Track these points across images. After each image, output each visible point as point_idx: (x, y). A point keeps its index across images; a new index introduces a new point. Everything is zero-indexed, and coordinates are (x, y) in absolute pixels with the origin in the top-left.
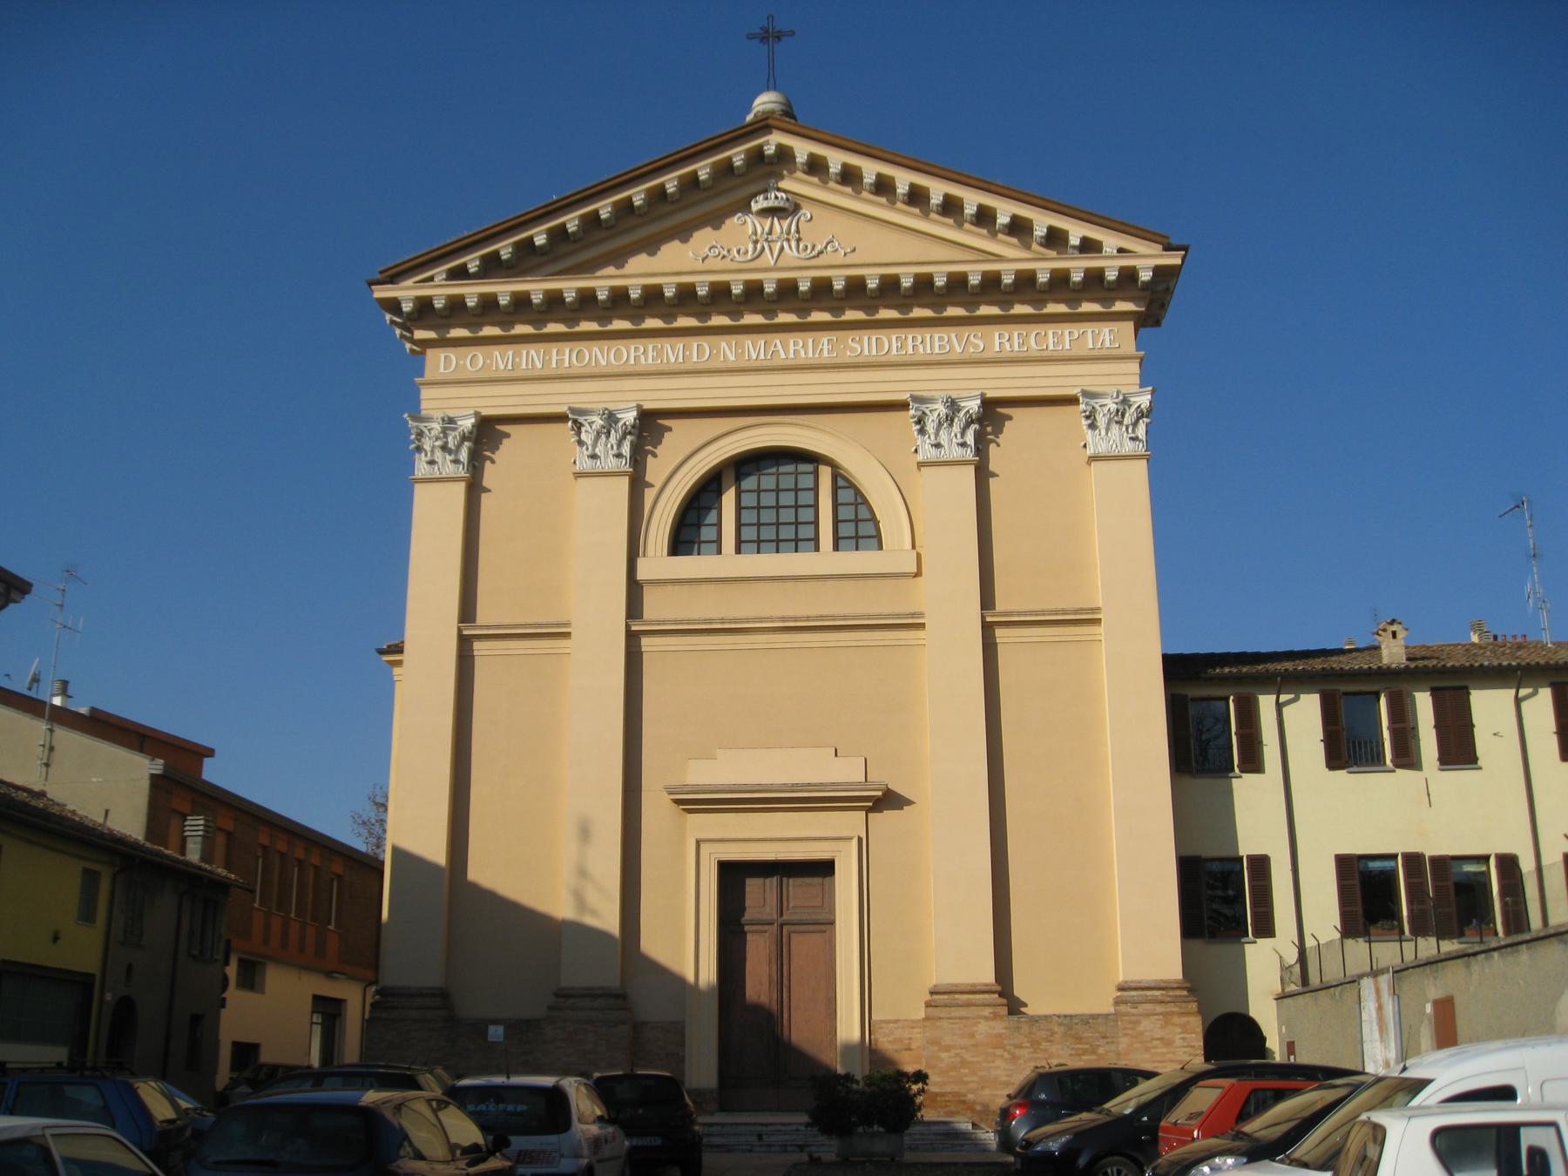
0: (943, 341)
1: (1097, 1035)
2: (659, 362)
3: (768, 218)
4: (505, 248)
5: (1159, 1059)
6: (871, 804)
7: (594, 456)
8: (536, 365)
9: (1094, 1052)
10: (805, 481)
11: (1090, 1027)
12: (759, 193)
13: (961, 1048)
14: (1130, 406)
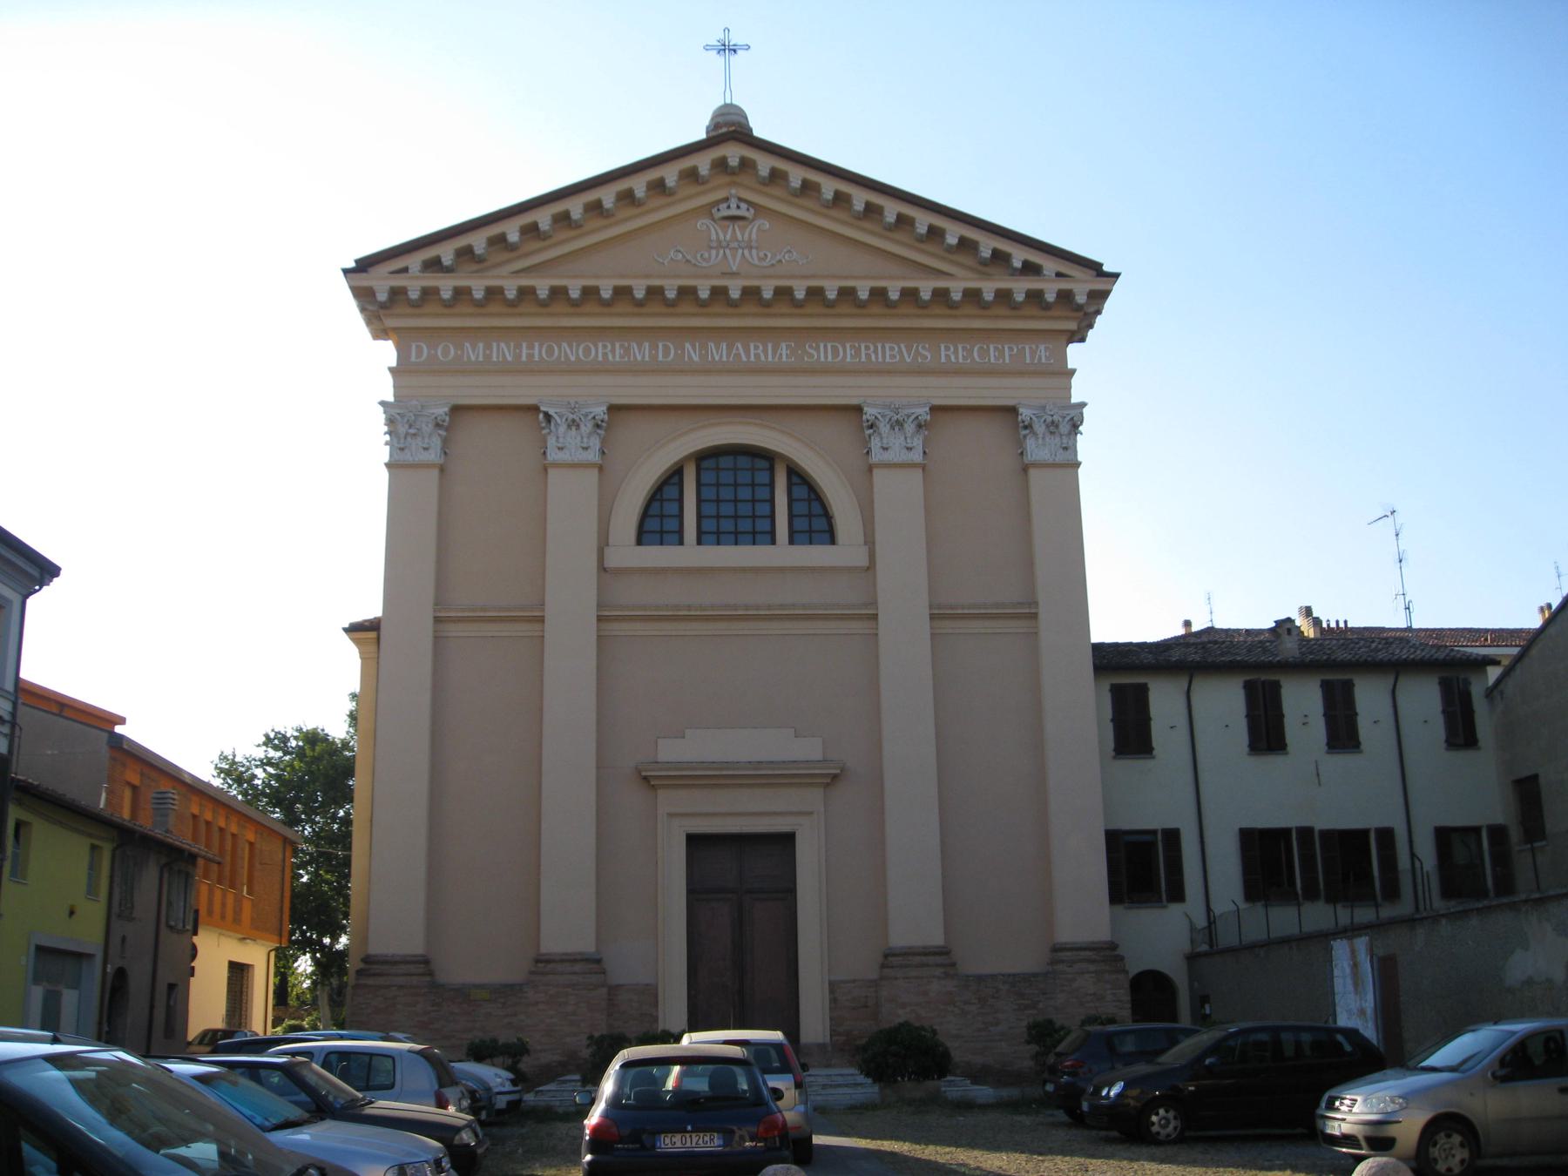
10: (763, 477)
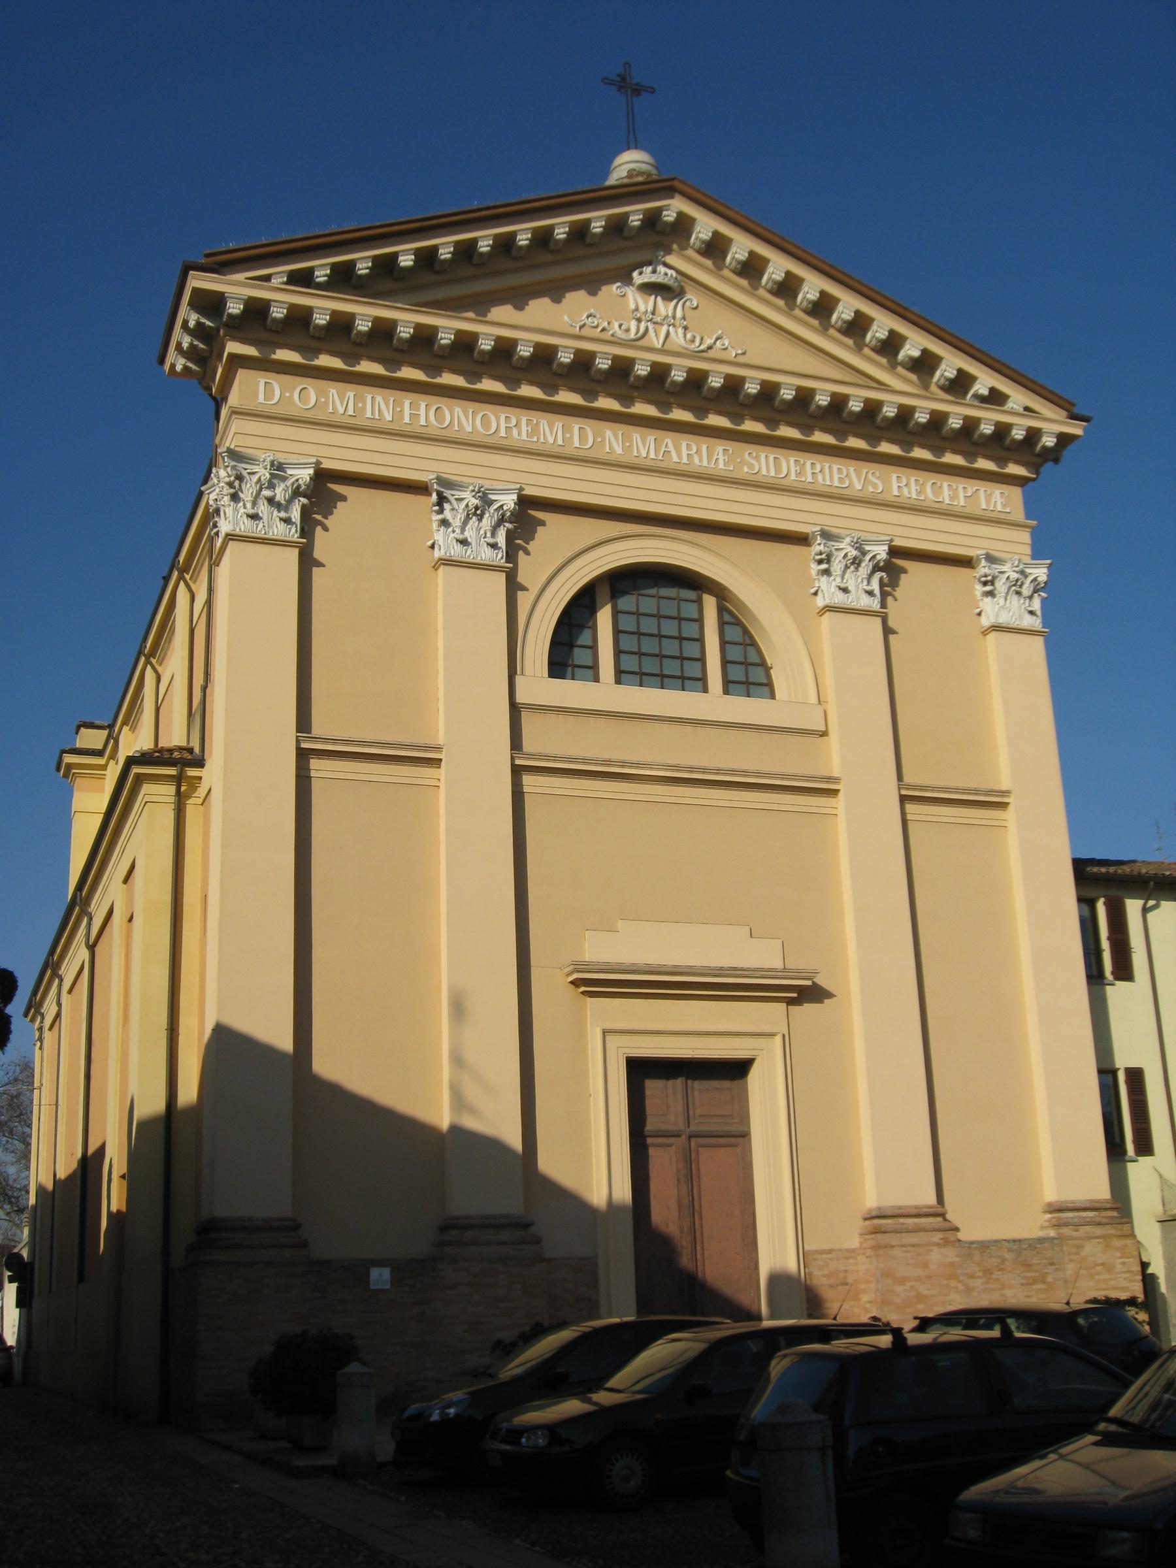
1: (1045, 1261)
2: (535, 439)
3: (651, 295)
4: (363, 261)
5: (1104, 1286)
6: (795, 995)
7: (464, 542)
9: (1044, 1282)
10: (690, 611)
11: (1038, 1253)
12: (649, 263)
13: (917, 1280)
14: (1026, 577)
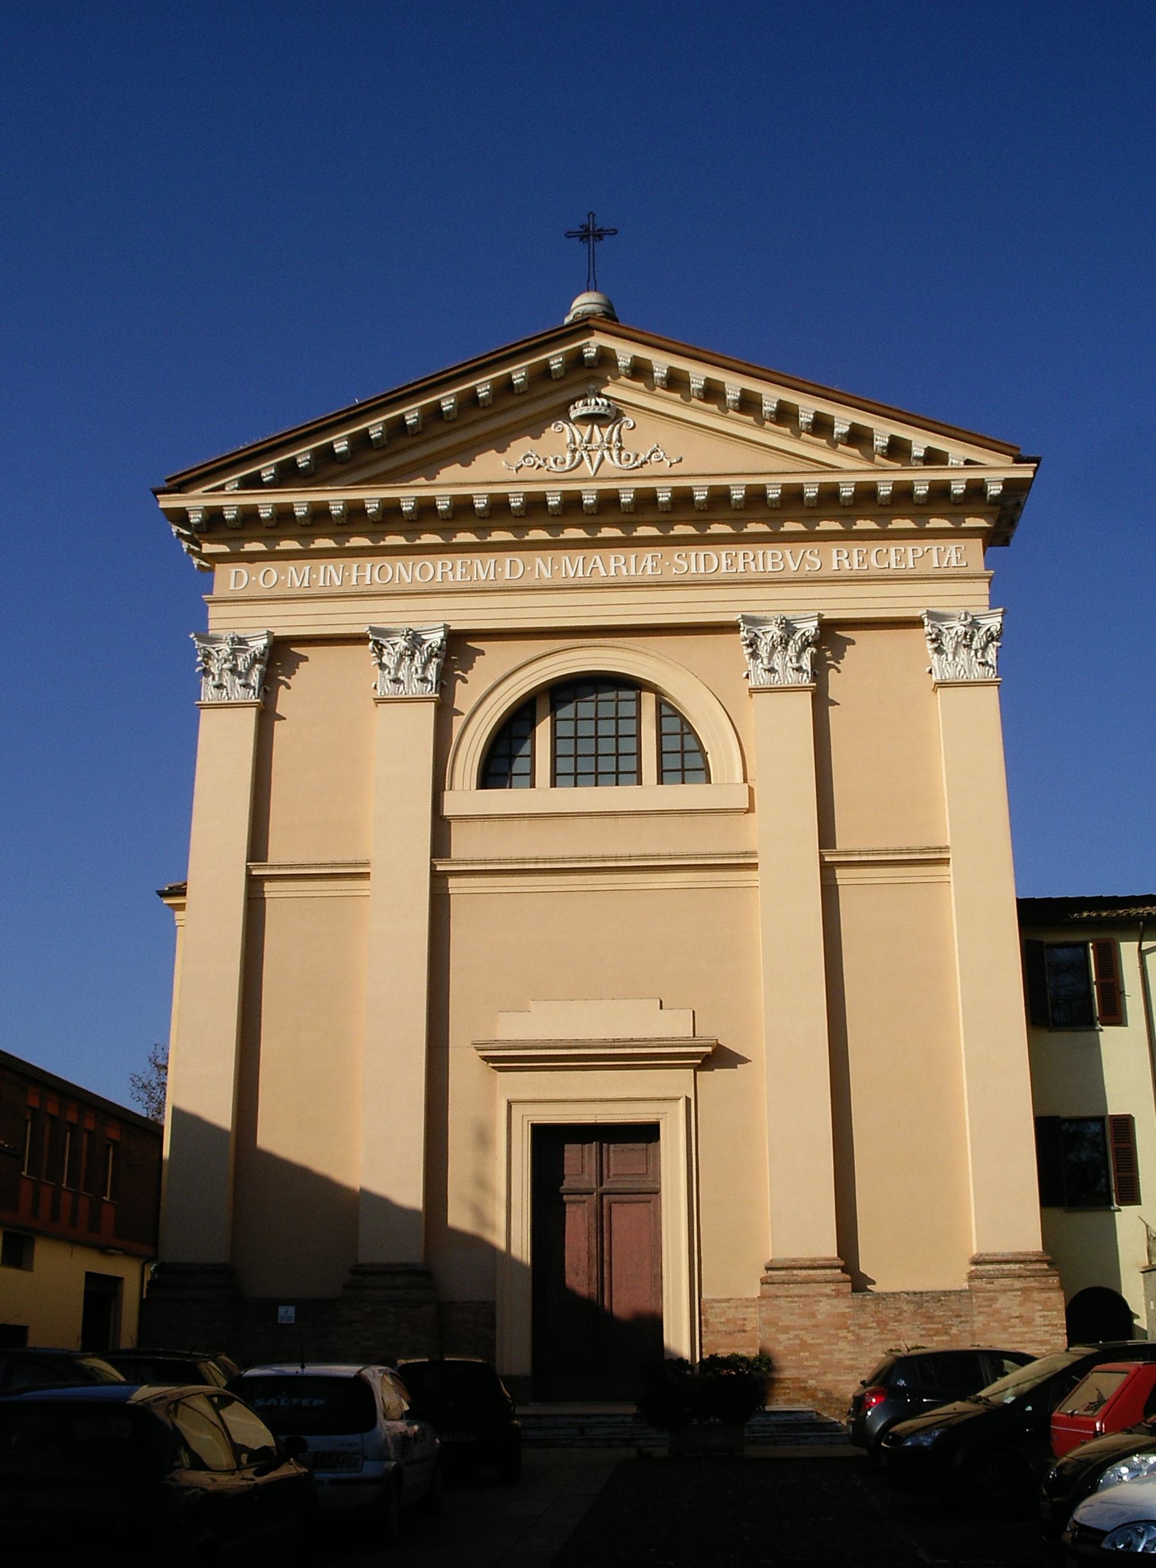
0: (842, 556)
1: (949, 1313)
2: (469, 579)
3: (588, 425)
4: (302, 456)
5: (1018, 1339)
6: (699, 1061)
7: (397, 681)
8: (404, 580)
9: (947, 1333)
10: (628, 709)
11: (942, 1304)
12: (579, 399)
13: (802, 1330)
14: (979, 629)
